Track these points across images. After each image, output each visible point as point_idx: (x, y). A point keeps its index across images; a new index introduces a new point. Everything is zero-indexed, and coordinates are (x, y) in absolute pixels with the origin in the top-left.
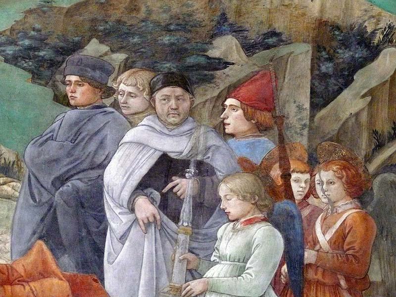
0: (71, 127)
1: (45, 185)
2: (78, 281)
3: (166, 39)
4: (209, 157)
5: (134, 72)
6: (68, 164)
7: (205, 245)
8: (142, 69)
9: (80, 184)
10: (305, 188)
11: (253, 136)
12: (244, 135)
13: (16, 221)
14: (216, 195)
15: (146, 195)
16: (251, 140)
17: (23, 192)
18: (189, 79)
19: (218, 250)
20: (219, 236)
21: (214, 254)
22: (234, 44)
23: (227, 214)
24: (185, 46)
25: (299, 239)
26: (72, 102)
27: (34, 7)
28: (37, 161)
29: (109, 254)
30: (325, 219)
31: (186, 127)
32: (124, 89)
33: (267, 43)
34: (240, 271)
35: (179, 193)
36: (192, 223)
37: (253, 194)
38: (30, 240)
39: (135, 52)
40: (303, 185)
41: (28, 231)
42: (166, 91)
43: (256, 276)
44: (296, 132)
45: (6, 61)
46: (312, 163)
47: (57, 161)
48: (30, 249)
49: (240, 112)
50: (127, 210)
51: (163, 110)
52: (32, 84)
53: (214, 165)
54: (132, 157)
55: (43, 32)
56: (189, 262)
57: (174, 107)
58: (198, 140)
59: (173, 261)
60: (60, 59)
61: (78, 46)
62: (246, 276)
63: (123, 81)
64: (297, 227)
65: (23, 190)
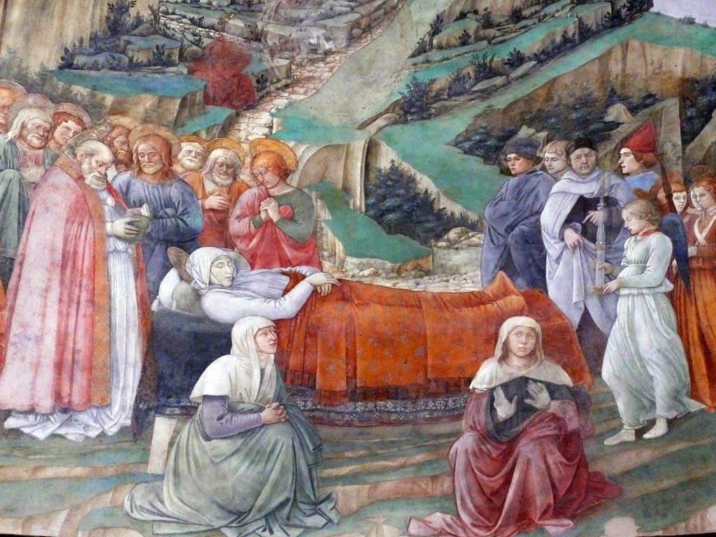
1: (500, 232)
3: (574, 116)
5: (555, 143)
8: (560, 140)
9: (525, 228)
10: (684, 203)
11: (643, 172)
12: (637, 172)
13: (483, 261)
16: (641, 175)
17: (486, 241)
20: (625, 247)
22: (622, 109)
23: (630, 231)
24: (588, 117)
26: (513, 172)
28: (494, 217)
29: (549, 273)
31: (595, 174)
33: (646, 104)
34: (643, 269)
35: (594, 222)
36: (606, 242)
38: (494, 272)
39: (554, 129)
40: (682, 200)
41: (492, 266)
42: (578, 152)
44: (673, 164)
45: (465, 153)
46: (687, 183)
47: (506, 215)
48: (494, 278)
49: (632, 156)
52: (483, 165)
54: (559, 203)
56: (606, 269)
57: (584, 162)
59: (595, 270)
60: (502, 144)
61: (513, 133)
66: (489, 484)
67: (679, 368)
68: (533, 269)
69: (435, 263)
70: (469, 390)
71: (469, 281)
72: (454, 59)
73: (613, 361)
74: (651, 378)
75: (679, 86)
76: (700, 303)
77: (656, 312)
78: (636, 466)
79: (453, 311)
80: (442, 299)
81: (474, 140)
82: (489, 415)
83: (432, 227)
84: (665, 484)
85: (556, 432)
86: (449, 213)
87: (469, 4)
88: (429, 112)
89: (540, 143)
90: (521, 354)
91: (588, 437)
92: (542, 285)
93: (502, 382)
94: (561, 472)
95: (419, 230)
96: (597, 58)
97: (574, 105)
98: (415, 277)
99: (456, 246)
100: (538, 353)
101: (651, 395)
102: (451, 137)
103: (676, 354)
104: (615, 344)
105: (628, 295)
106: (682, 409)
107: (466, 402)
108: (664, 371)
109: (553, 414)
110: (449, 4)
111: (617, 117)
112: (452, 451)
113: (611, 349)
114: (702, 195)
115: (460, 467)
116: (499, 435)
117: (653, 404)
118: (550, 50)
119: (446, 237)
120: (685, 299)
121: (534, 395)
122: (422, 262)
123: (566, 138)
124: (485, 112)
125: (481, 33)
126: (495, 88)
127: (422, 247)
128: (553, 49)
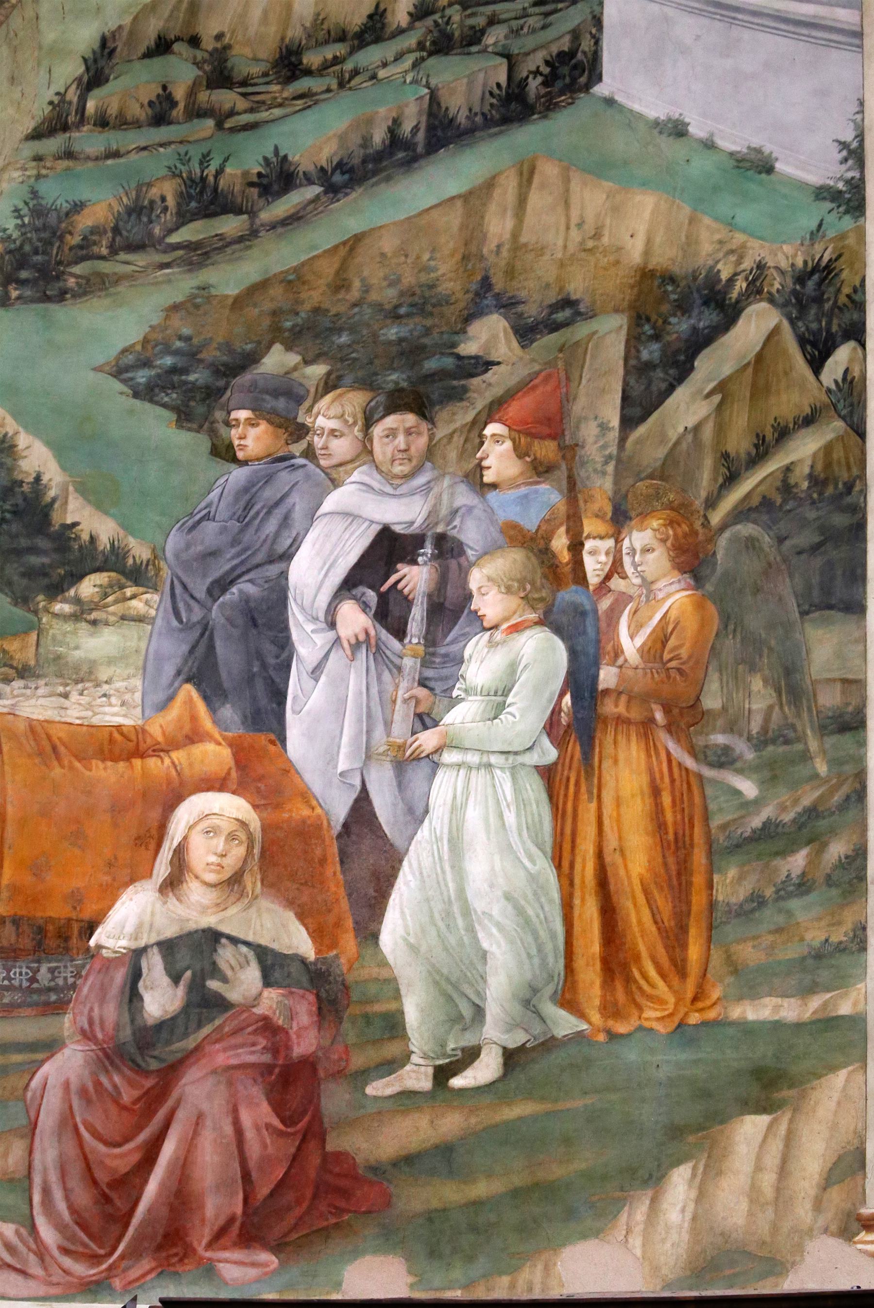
1: (198, 595)
2: (246, 745)
3: (392, 332)
4: (455, 527)
5: (340, 395)
6: (233, 558)
7: (445, 672)
8: (353, 388)
9: (251, 589)
10: (606, 564)
12: (513, 484)
13: (151, 657)
14: (465, 589)
15: (354, 598)
16: (524, 490)
17: (162, 609)
18: (428, 397)
19: (464, 679)
20: (466, 655)
21: (458, 686)
23: (481, 618)
24: (426, 341)
25: (592, 650)
26: (240, 455)
27: (180, 298)
28: (184, 556)
30: (635, 612)
31: (421, 480)
32: (323, 425)
33: (555, 322)
35: (406, 591)
36: (425, 638)
37: (522, 582)
38: (171, 684)
39: (342, 360)
40: (603, 558)
41: (169, 670)
42: (391, 421)
43: (521, 716)
45: (136, 395)
47: (213, 554)
48: (171, 698)
49: (508, 444)
50: (324, 625)
51: (384, 453)
52: (177, 431)
53: (463, 538)
54: (334, 538)
55: (195, 341)
56: (418, 702)
57: (403, 446)
58: (439, 497)
60: (221, 383)
61: (252, 359)
64: (591, 631)
65: (163, 605)
66: (108, 1161)
67: (543, 934)
69: (41, 650)
70: (88, 949)
71: (113, 700)
72: (133, 157)
73: (407, 912)
74: (484, 955)
76: (608, 797)
77: (513, 808)
78: (428, 1145)
79: (71, 768)
80: (49, 737)
81: (160, 367)
82: (126, 1008)
83: (43, 564)
84: (481, 1189)
85: (267, 1058)
86: (85, 537)
87: (181, 15)
88: (61, 284)
89: (308, 391)
90: (211, 877)
91: (333, 1075)
92: (275, 725)
93: (162, 937)
94: (265, 1146)
96: (459, 196)
97: (396, 307)
99: (94, 615)
100: (248, 879)
101: (478, 994)
102: (107, 353)
103: (542, 908)
104: (417, 874)
105: (459, 766)
106: (537, 1029)
107: (78, 975)
108: (512, 942)
109: (265, 1018)
110: (135, 10)
111: (487, 346)
112: (36, 1083)
114: (646, 550)
115: (48, 1120)
116: (142, 1055)
117: (479, 1012)
118: (356, 161)
119: (72, 592)
120: (577, 784)
121: (229, 973)
123: (367, 384)
124: (193, 297)
125: (203, 96)
126: (221, 244)
127: (19, 612)
128: (364, 162)
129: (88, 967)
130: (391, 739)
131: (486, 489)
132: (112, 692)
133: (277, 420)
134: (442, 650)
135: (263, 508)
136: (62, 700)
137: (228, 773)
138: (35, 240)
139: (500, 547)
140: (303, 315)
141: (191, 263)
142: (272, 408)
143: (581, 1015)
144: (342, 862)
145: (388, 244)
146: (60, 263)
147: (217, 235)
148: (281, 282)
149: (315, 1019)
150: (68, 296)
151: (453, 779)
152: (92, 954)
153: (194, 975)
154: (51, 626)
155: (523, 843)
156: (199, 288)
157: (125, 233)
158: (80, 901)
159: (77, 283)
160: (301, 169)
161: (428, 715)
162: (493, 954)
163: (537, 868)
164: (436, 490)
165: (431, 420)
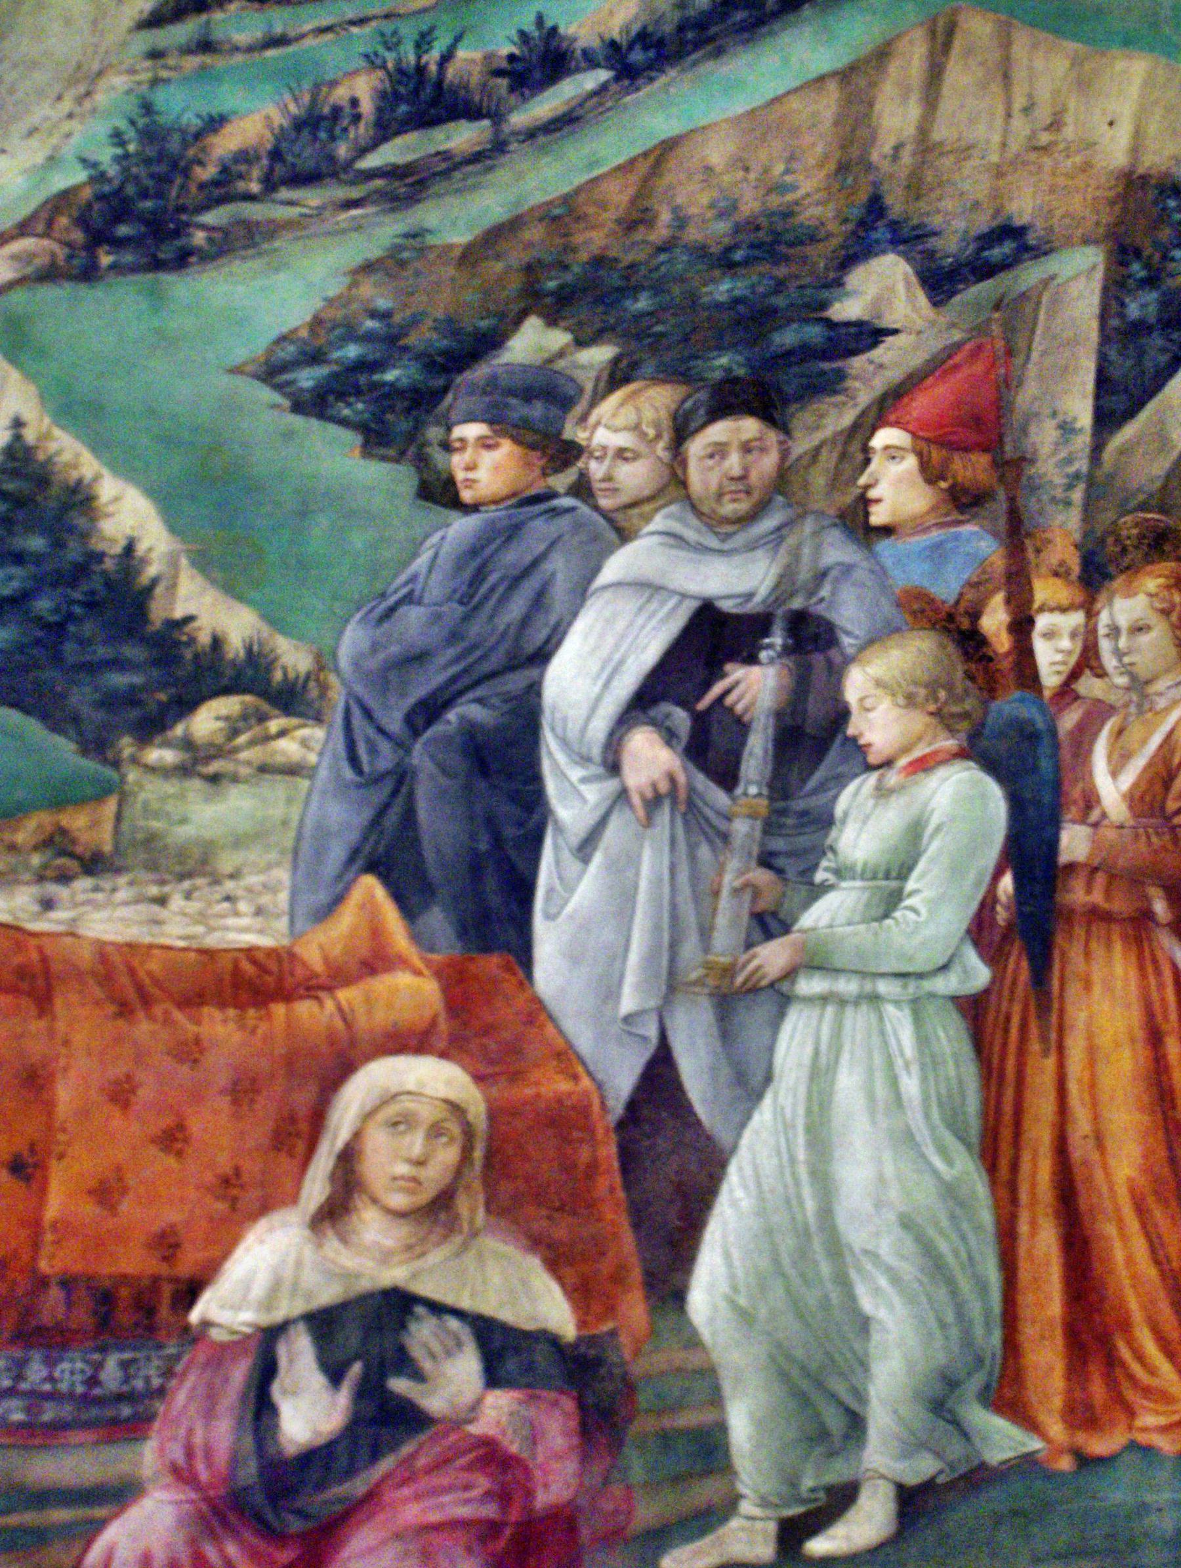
0: (459, 565)
3: (723, 289)
7: (802, 841)
8: (656, 380)
18: (780, 391)
22: (900, 277)
24: (780, 301)
26: (466, 496)
27: (375, 253)
31: (768, 523)
32: (604, 441)
34: (891, 901)
36: (770, 786)
37: (932, 686)
38: (339, 877)
39: (638, 337)
41: (337, 852)
42: (719, 431)
43: (931, 912)
45: (298, 407)
47: (417, 658)
48: (338, 900)
49: (911, 462)
50: (600, 770)
51: (706, 483)
52: (362, 462)
53: (832, 616)
54: (620, 625)
55: (397, 318)
57: (736, 471)
58: (796, 555)
59: (716, 893)
60: (440, 382)
61: (492, 341)
62: (904, 916)
63: (604, 421)
65: (330, 746)
67: (965, 1286)
68: (491, 883)
69: (125, 826)
71: (242, 906)
72: (309, 42)
73: (736, 1254)
74: (864, 1324)
75: (1112, 203)
77: (915, 1069)
79: (168, 1021)
80: (132, 972)
81: (337, 362)
83: (133, 688)
85: (490, 1511)
86: (204, 639)
89: (581, 390)
90: (399, 1201)
95: (81, 697)
96: (834, 74)
97: (729, 249)
98: (40, 879)
99: (214, 767)
100: (463, 1204)
103: (963, 1238)
104: (752, 1186)
105: (824, 999)
106: (956, 1449)
111: (877, 302)
113: (734, 1203)
117: (856, 1423)
118: (668, 28)
119: (179, 730)
121: (427, 1365)
122: (77, 821)
126: (444, 165)
127: (90, 765)
128: (681, 28)
129: (186, 1358)
130: (711, 958)
131: (873, 535)
132: (240, 893)
133: (530, 438)
134: (799, 805)
135: (502, 579)
136: (156, 908)
137: (434, 1023)
138: (143, 175)
139: (898, 630)
140: (576, 269)
141: (396, 198)
142: (521, 418)
143: (1031, 1425)
144: (625, 1170)
145: (717, 153)
146: (182, 209)
147: (438, 153)
148: (541, 220)
149: (575, 1441)
150: (193, 259)
151: (814, 1022)
152: (194, 1336)
153: (367, 1367)
154: (141, 787)
155: (932, 1129)
156: (406, 236)
157: (290, 158)
158: (176, 1246)
159: (210, 240)
160: (580, 45)
161: (774, 914)
162: (879, 1322)
163: (954, 1172)
164: (791, 541)
165: (784, 428)
